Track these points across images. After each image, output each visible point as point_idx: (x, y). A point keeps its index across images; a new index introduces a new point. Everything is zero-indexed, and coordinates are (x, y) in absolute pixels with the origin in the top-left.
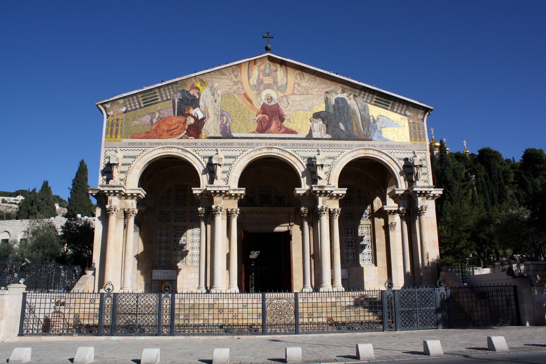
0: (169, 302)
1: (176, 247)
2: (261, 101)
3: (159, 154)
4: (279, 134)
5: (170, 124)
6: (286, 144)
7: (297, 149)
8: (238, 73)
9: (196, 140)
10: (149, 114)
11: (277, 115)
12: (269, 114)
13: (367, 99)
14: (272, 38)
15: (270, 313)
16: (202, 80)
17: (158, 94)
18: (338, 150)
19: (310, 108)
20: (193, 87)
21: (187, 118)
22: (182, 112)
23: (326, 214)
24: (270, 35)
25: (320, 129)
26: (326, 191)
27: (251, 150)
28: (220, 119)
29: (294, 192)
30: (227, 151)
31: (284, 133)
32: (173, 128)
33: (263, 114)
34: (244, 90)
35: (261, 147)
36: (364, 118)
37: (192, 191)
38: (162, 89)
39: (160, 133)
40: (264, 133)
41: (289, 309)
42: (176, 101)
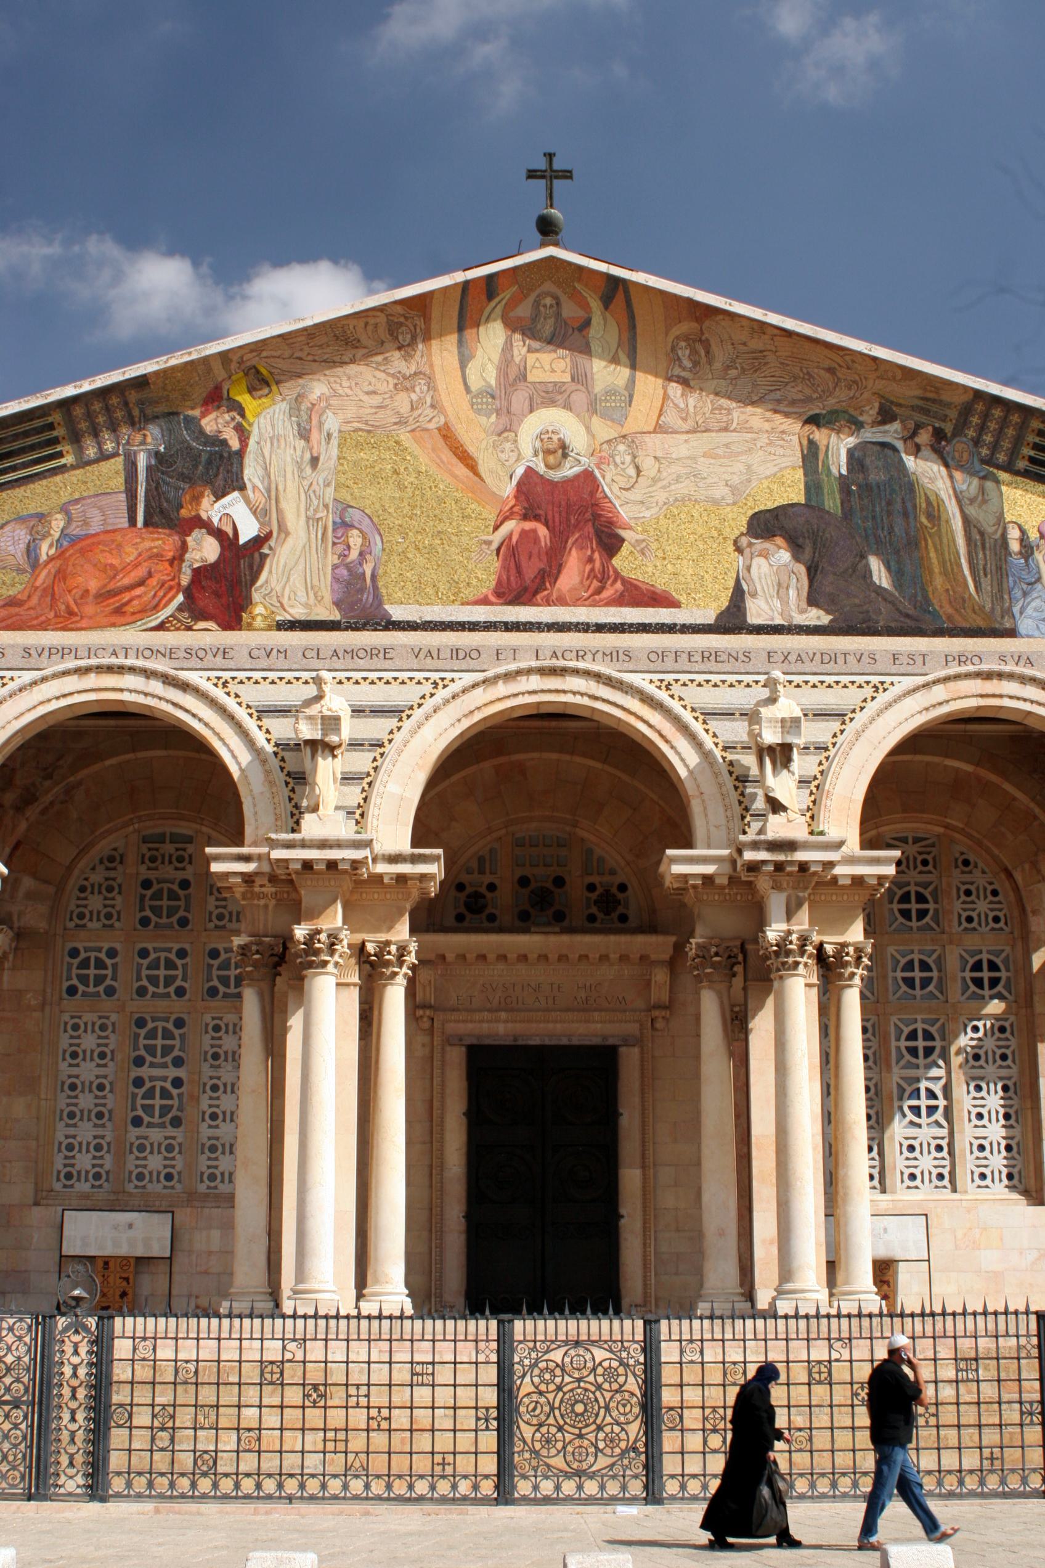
0: (90, 1353)
1: (140, 1112)
2: (518, 460)
3: (64, 696)
5: (111, 565)
6: (627, 653)
7: (677, 676)
9: (229, 634)
10: (21, 519)
12: (550, 517)
13: (995, 447)
14: (571, 177)
15: (534, 1409)
16: (255, 367)
17: (59, 432)
18: (860, 679)
19: (734, 490)
21: (189, 539)
23: (801, 966)
24: (557, 166)
25: (781, 588)
26: (803, 867)
27: (469, 678)
28: (334, 544)
29: (662, 868)
30: (365, 686)
31: (619, 601)
32: (126, 581)
33: (525, 517)
34: (442, 411)
35: (513, 667)
36: (982, 534)
37: (208, 860)
39: (68, 607)
41: (617, 1391)
42: (142, 461)
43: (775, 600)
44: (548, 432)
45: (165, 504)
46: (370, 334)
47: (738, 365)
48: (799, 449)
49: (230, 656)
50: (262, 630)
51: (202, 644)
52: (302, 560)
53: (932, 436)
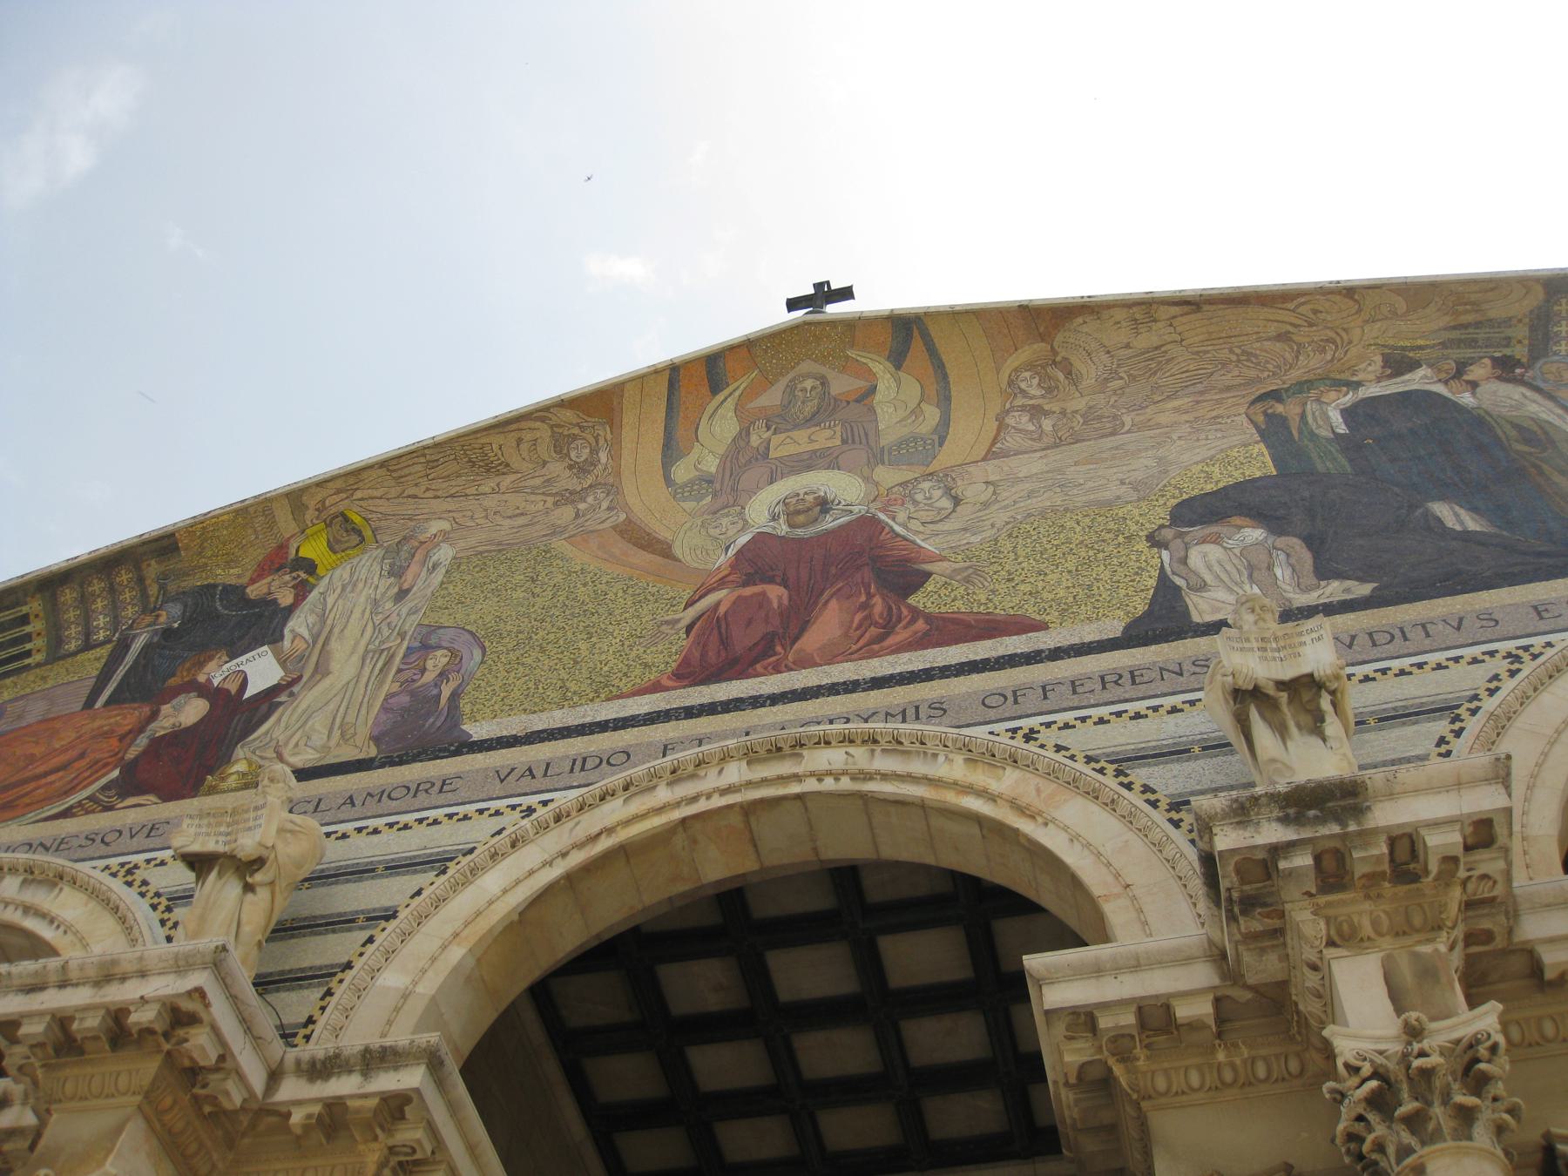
4: (875, 662)
5: (33, 755)
6: (939, 709)
8: (594, 451)
9: (171, 805)
11: (859, 568)
16: (343, 514)
17: (35, 626)
20: (279, 561)
28: (399, 671)
33: (745, 584)
38: (68, 595)
40: (742, 675)
43: (1247, 587)
44: (798, 495)
45: (149, 677)
46: (525, 454)
47: (1122, 375)
48: (1251, 426)
49: (160, 832)
50: (232, 790)
51: (118, 826)
52: (338, 698)
53: (1494, 368)
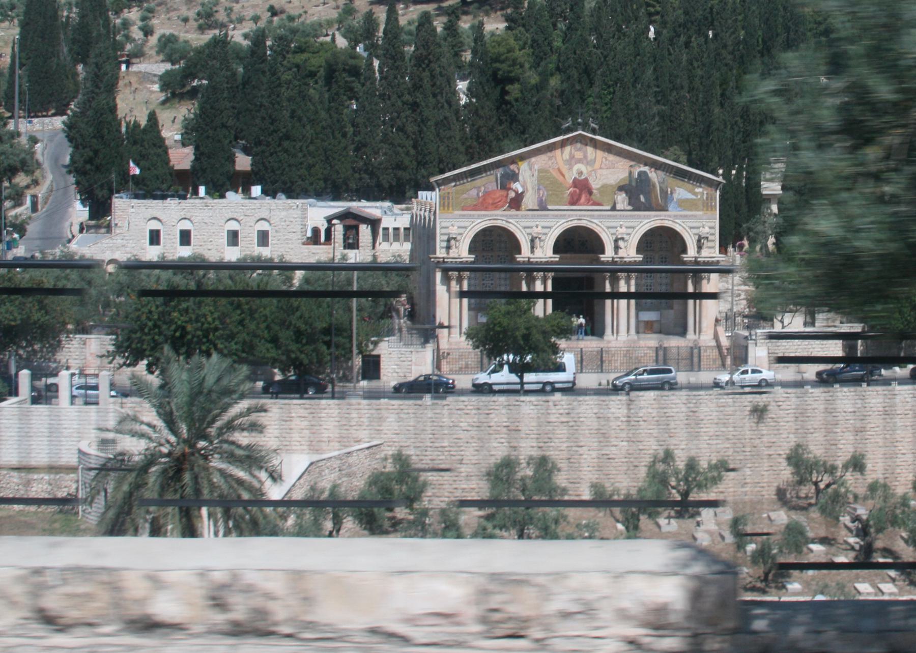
22: (504, 187)
25: (623, 202)
27: (564, 221)
42: (499, 175)
